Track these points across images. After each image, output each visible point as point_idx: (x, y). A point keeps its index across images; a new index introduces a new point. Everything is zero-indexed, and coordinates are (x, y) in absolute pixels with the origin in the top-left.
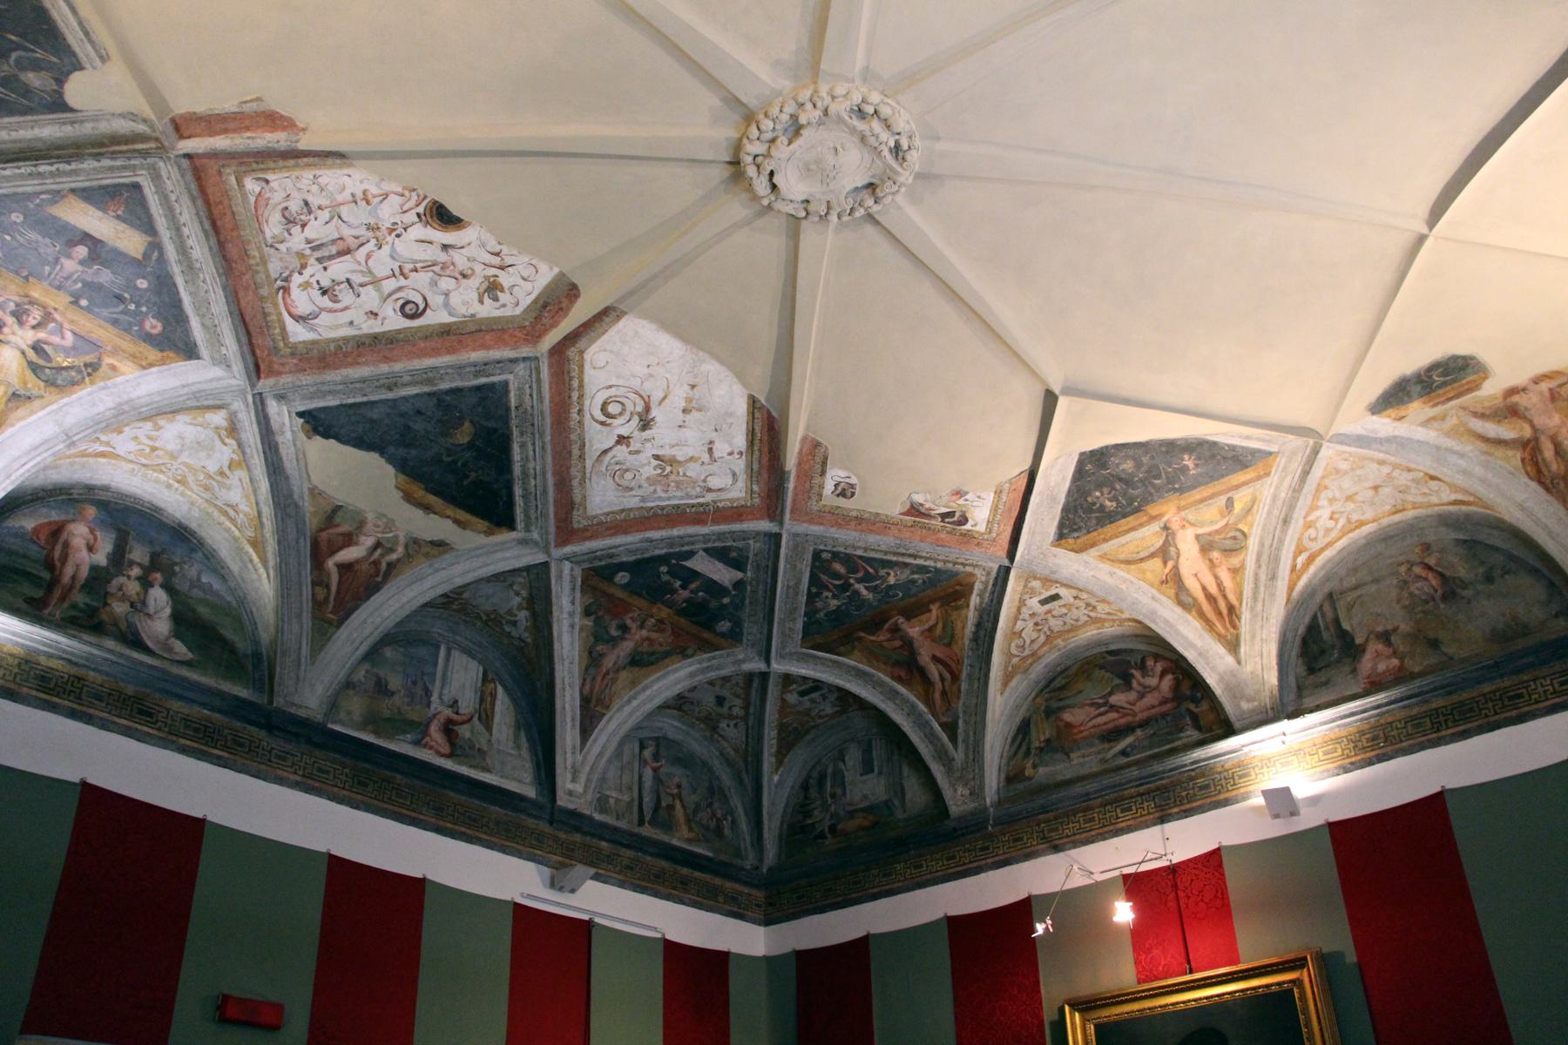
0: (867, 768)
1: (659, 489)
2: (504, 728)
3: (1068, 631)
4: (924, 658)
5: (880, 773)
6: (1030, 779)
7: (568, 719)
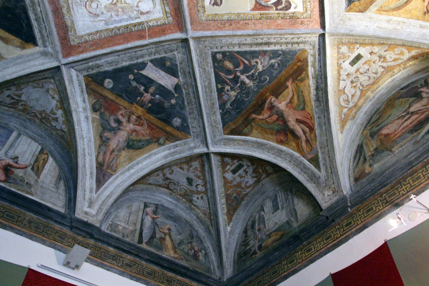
0: (276, 208)
1: (113, 14)
2: (49, 178)
3: (373, 84)
4: (292, 123)
5: (282, 208)
6: (369, 173)
7: (88, 173)
